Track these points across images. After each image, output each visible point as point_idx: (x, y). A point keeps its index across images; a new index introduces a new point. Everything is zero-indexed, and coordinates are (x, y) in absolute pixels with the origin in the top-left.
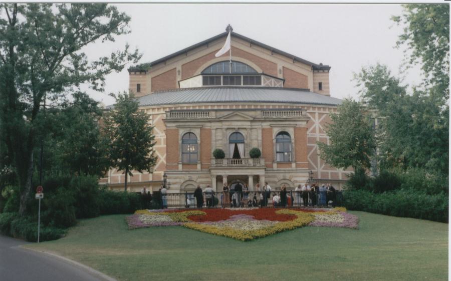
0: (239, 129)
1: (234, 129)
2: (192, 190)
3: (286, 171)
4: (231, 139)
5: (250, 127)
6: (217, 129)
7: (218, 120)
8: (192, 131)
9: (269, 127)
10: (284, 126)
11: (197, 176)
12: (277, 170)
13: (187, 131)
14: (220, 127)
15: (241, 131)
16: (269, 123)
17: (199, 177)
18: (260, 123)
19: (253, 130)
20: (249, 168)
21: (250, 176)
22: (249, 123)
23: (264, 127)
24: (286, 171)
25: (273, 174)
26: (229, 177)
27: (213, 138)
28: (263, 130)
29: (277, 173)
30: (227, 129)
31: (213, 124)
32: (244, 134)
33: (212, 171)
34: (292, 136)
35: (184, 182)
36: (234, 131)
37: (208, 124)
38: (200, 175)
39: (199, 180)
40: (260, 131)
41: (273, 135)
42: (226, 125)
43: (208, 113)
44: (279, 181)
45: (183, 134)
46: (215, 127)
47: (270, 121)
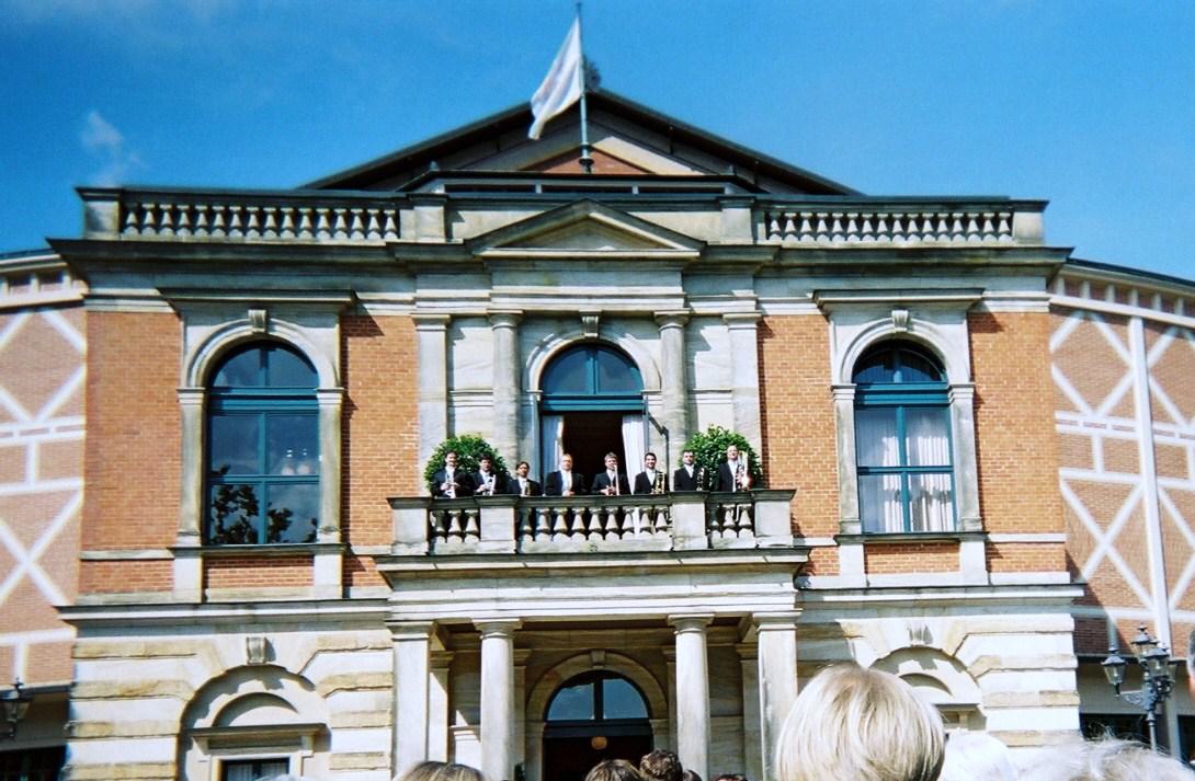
0: (607, 318)
1: (574, 317)
3: (925, 596)
5: (677, 306)
7: (463, 262)
10: (901, 305)
12: (866, 590)
20: (676, 565)
24: (925, 596)
26: (528, 637)
27: (431, 377)
34: (956, 372)
40: (750, 334)
41: (836, 360)
42: (513, 296)
43: (397, 219)
46: (445, 310)
47: (812, 271)
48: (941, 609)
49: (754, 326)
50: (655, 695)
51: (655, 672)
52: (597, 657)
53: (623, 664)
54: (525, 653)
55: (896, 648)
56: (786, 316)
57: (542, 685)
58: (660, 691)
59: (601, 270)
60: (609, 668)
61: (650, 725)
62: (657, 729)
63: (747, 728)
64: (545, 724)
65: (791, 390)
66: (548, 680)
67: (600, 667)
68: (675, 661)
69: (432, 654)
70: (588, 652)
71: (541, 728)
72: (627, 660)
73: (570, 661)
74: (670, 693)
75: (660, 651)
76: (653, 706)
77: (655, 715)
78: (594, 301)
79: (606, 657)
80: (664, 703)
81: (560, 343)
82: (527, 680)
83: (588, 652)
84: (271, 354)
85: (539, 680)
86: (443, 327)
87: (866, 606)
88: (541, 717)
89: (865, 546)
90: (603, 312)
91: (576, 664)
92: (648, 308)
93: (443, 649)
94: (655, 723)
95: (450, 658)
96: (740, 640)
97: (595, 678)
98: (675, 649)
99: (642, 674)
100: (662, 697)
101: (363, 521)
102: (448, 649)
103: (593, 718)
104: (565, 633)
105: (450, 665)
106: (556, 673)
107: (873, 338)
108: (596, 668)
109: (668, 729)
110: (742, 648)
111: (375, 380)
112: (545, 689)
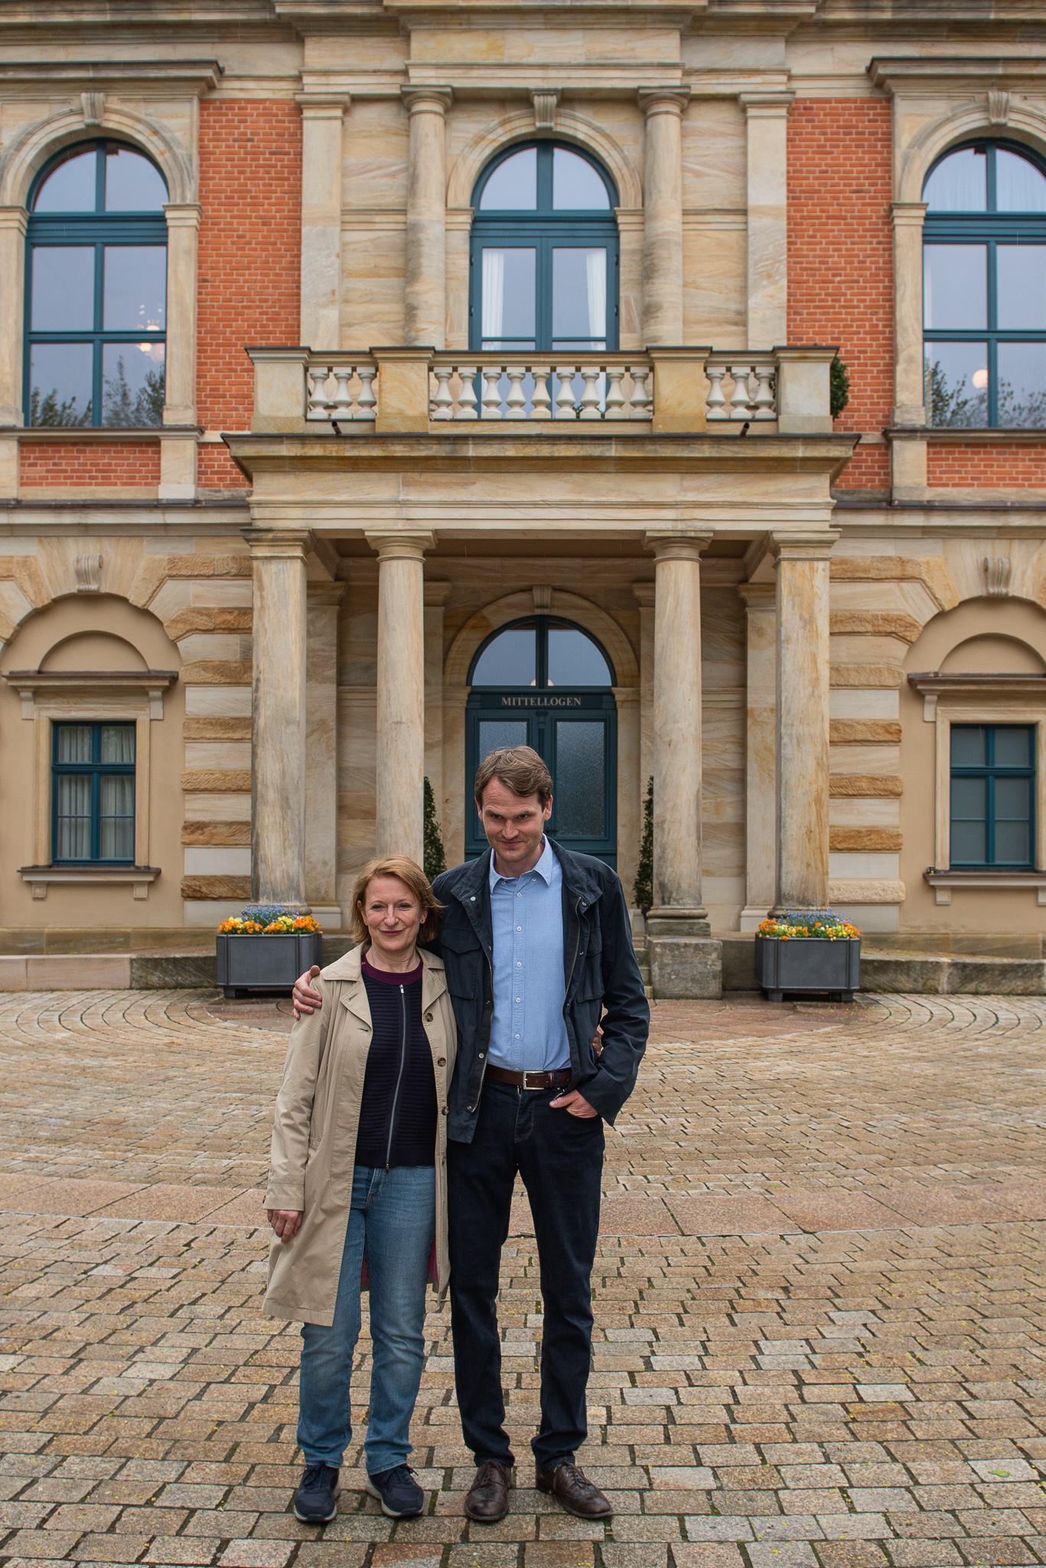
0: (568, 99)
1: (521, 99)
2: (163, 678)
3: (1016, 520)
4: (491, 201)
5: (673, 79)
6: (358, 100)
8: (113, 122)
9: (856, 90)
11: (155, 554)
13: (75, 124)
14: (389, 86)
15: (578, 125)
16: (856, 56)
17: (175, 573)
18: (769, 53)
19: (705, 118)
21: (666, 542)
22: (665, 46)
23: (805, 90)
25: (888, 549)
28: (797, 110)
29: (927, 532)
30: (458, 101)
31: (319, 53)
32: (612, 159)
33: (267, 488)
35: (39, 614)
36: (521, 125)
37: (276, 59)
38: (185, 550)
39: (171, 600)
44: (942, 615)
45: (29, 155)
48: (1039, 542)
49: (783, 112)
50: (622, 655)
51: (621, 621)
52: (541, 596)
53: (577, 607)
54: (442, 589)
55: (967, 597)
56: (828, 101)
57: (464, 634)
58: (627, 646)
59: (562, 28)
60: (556, 612)
61: (613, 695)
62: (623, 702)
63: (749, 705)
64: (469, 689)
65: (833, 210)
66: (473, 627)
67: (546, 612)
68: (654, 606)
69: (312, 587)
70: (529, 589)
71: (463, 695)
72: (585, 603)
73: (502, 602)
74: (643, 651)
75: (630, 591)
76: (618, 669)
77: (620, 681)
78: (553, 73)
79: (552, 598)
80: (634, 667)
81: (502, 136)
82: (446, 627)
83: (529, 589)
84: (111, 160)
85: (460, 628)
86: (338, 113)
87: (927, 532)
88: (464, 678)
89: (929, 445)
90: (563, 90)
91: (510, 606)
92: (634, 85)
93: (331, 579)
94: (620, 694)
95: (338, 593)
96: (745, 580)
97: (542, 624)
98: (654, 589)
99: (599, 621)
100: (631, 655)
101: (224, 396)
102: (337, 579)
103: (534, 684)
104: (497, 562)
105: (342, 603)
106: (485, 618)
107: (956, 133)
108: (538, 612)
109: (638, 701)
110: (748, 590)
111: (243, 192)
112: (468, 640)
